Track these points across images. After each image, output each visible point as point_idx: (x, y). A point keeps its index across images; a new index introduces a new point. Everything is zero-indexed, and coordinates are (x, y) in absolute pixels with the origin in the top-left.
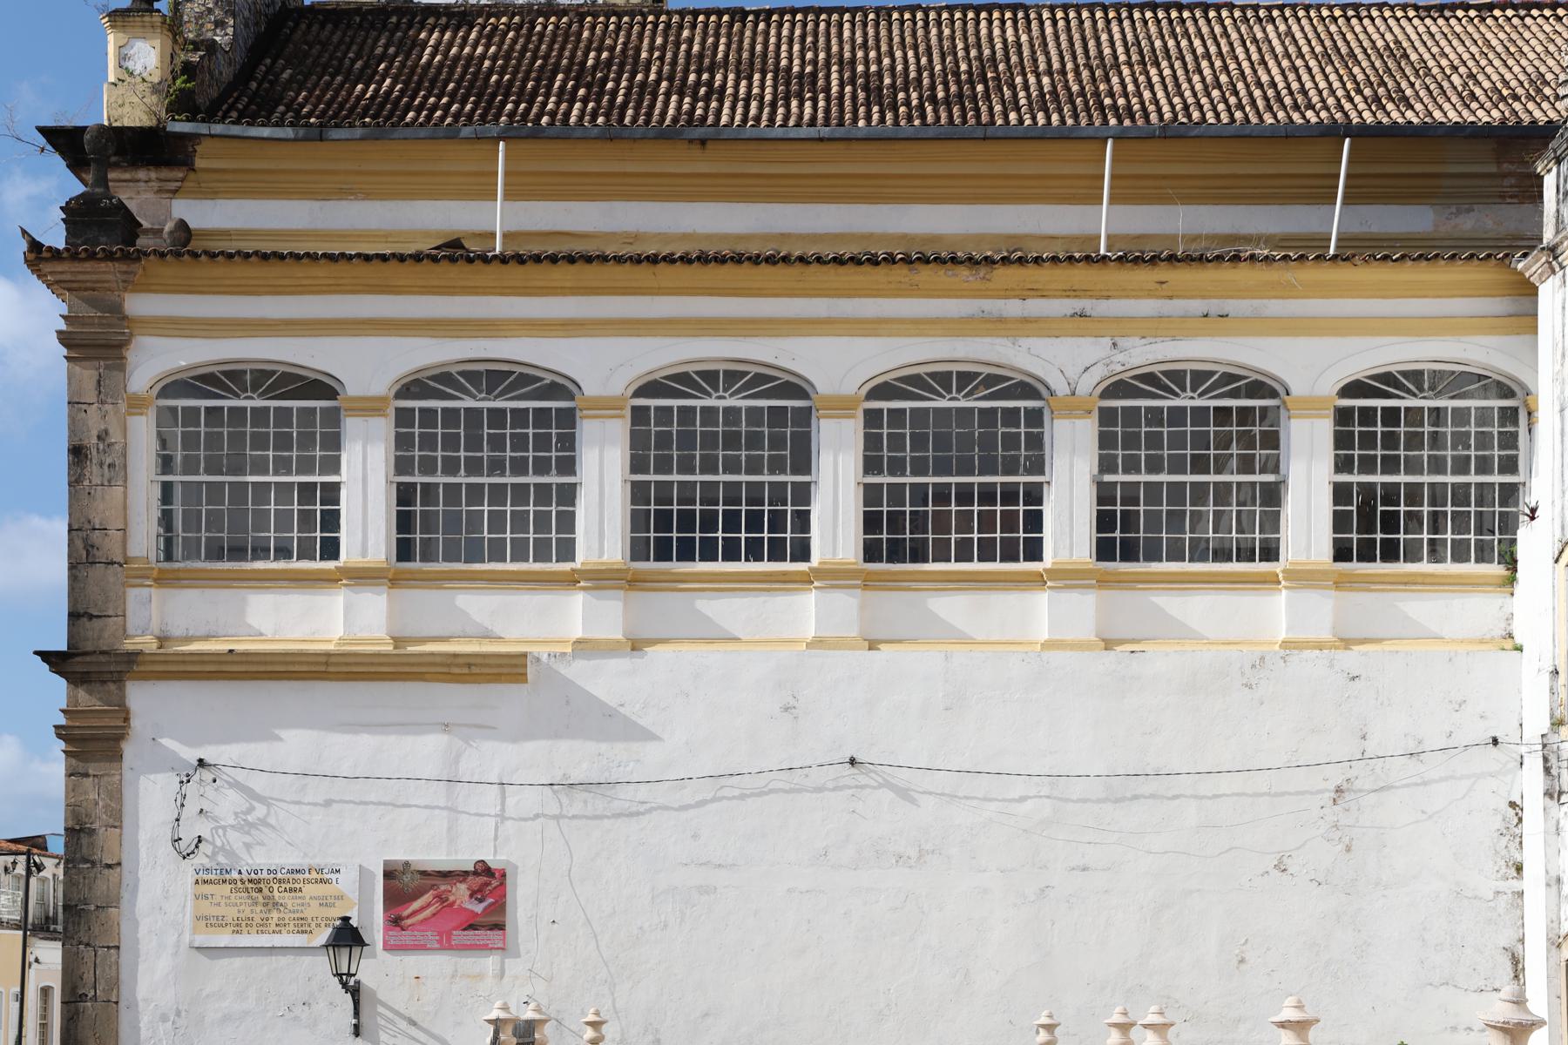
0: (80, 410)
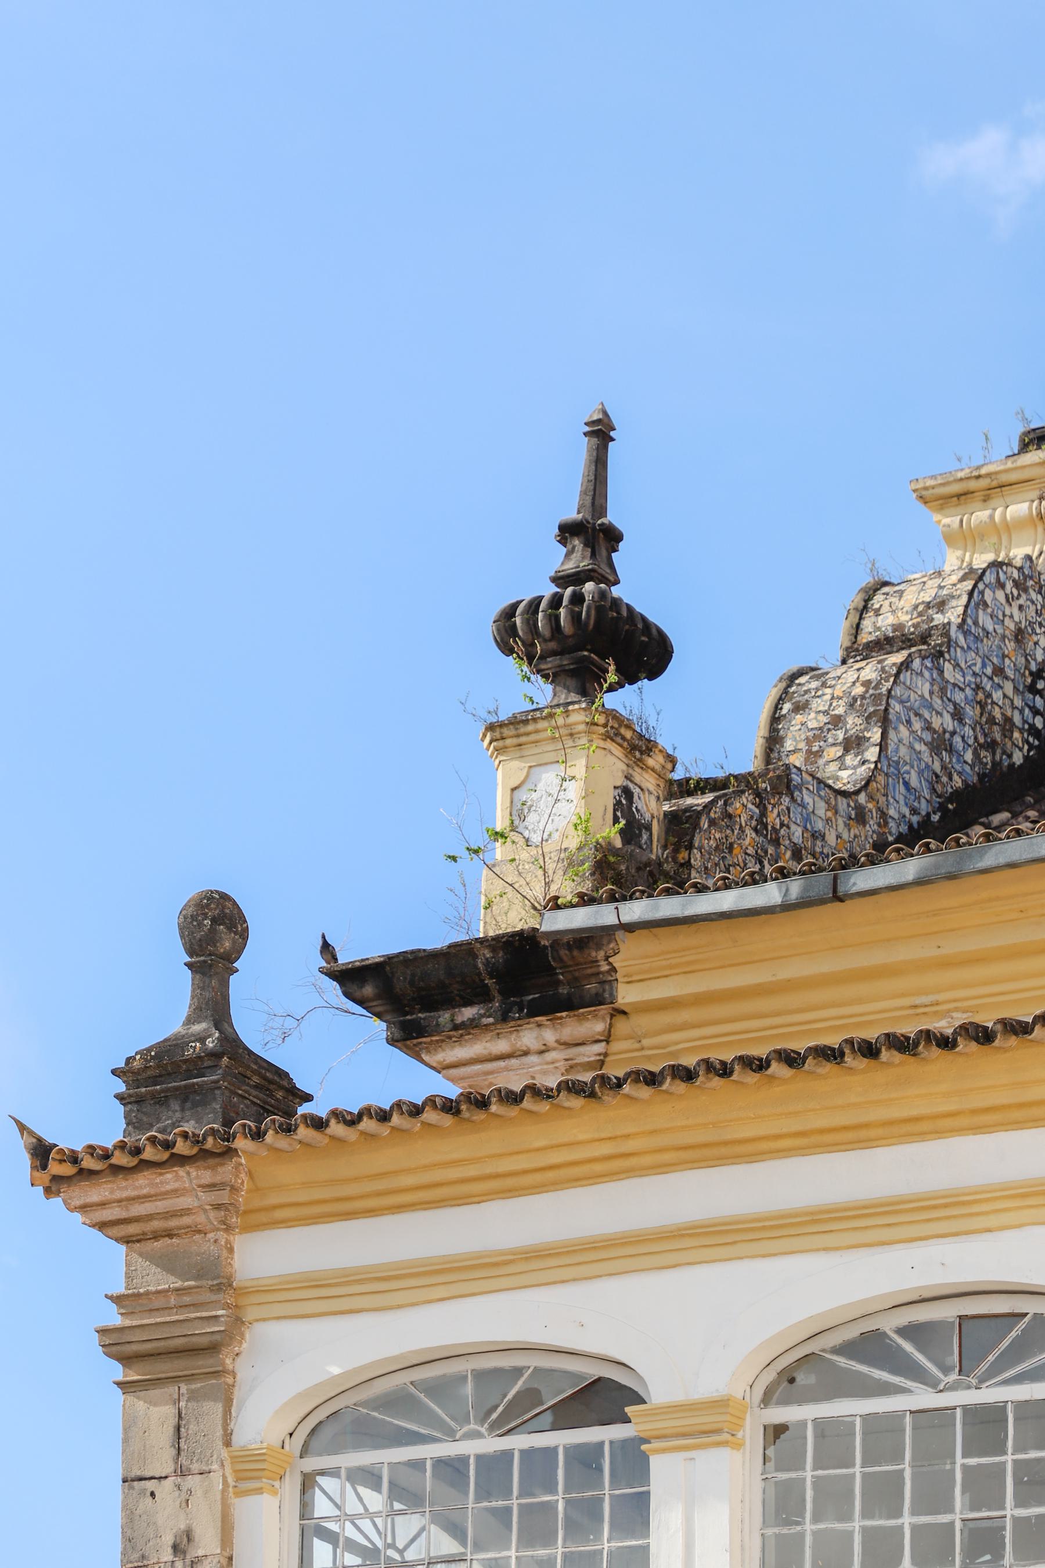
0: (143, 1492)
